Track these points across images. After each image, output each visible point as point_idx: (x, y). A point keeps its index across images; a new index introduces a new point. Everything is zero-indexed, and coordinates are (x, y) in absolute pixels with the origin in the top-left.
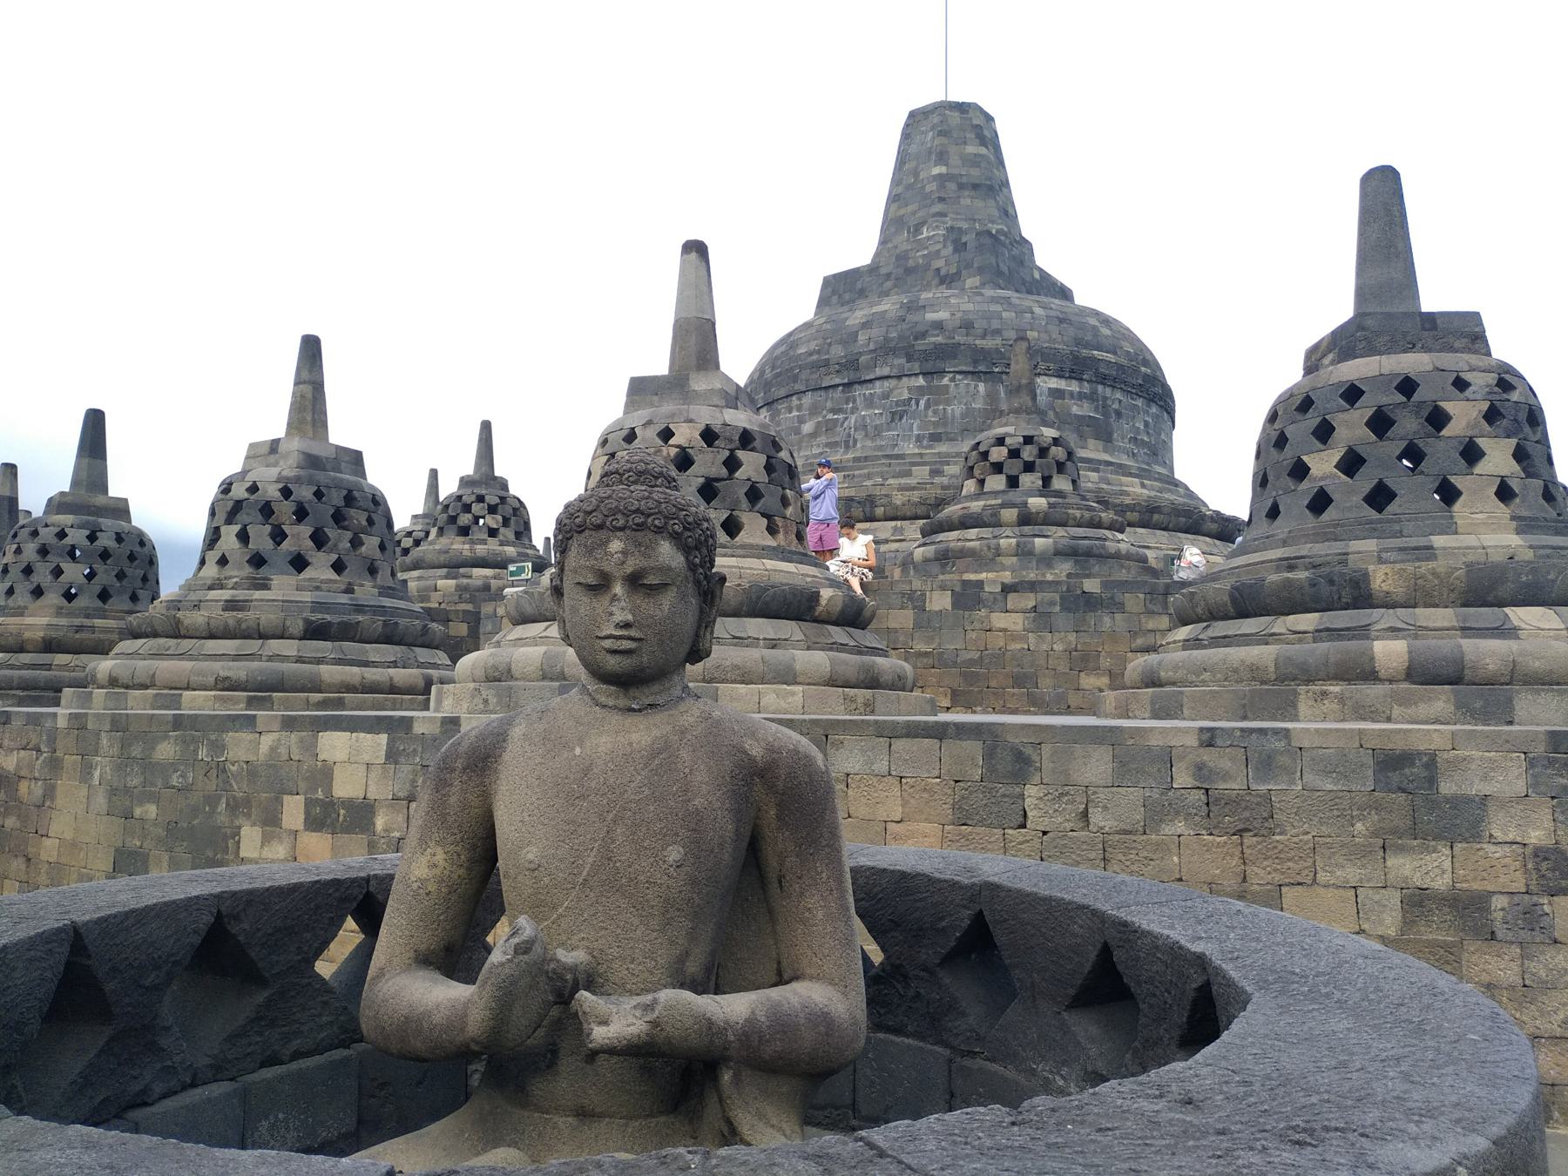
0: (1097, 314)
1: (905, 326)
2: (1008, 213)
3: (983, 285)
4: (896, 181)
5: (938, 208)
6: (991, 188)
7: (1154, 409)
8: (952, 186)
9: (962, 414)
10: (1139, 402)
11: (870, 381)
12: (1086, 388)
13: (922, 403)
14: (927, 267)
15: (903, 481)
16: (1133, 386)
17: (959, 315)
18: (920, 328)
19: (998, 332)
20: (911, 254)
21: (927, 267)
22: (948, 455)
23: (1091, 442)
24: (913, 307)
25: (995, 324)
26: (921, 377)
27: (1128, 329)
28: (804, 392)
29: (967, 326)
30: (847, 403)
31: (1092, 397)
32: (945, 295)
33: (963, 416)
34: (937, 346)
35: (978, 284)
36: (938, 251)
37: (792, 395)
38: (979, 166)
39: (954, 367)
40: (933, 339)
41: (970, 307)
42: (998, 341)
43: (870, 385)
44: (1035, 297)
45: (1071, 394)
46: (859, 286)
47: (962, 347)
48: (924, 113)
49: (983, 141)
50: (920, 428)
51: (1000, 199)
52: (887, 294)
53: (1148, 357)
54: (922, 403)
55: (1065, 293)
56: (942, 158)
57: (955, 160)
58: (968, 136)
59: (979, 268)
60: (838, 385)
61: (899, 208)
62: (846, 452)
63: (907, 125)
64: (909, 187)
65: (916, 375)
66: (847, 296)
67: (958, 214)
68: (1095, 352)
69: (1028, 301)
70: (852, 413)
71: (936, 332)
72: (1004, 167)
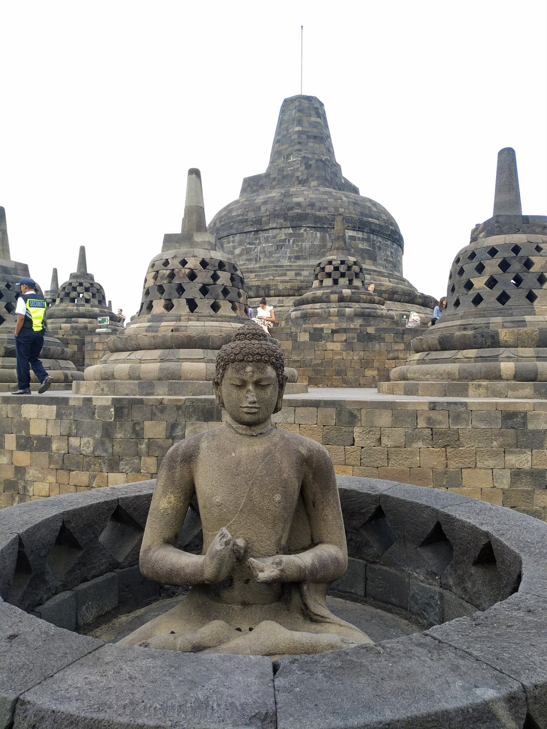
0: (370, 201)
2: (330, 151)
3: (319, 185)
4: (278, 133)
5: (297, 147)
6: (322, 138)
7: (395, 246)
8: (304, 137)
9: (309, 247)
10: (389, 243)
11: (267, 230)
13: (291, 241)
14: (292, 176)
15: (283, 278)
16: (386, 235)
17: (308, 200)
19: (326, 208)
20: (285, 169)
21: (292, 176)
22: (303, 266)
23: (367, 261)
24: (287, 195)
25: (325, 205)
26: (291, 228)
27: (384, 208)
28: (236, 234)
29: (312, 205)
30: (256, 240)
31: (368, 240)
32: (301, 190)
33: (310, 248)
34: (298, 214)
35: (317, 185)
36: (298, 168)
37: (230, 235)
39: (305, 224)
40: (296, 211)
41: (313, 196)
42: (326, 213)
43: (267, 232)
44: (343, 192)
45: (359, 238)
46: (260, 183)
50: (290, 253)
52: (273, 188)
53: (393, 222)
54: (291, 241)
55: (355, 190)
56: (300, 123)
57: (306, 124)
58: (312, 112)
59: (317, 177)
60: (251, 232)
61: (279, 146)
62: (256, 264)
63: (283, 106)
64: (284, 136)
65: (289, 227)
66: (255, 188)
69: (340, 194)
70: (259, 245)
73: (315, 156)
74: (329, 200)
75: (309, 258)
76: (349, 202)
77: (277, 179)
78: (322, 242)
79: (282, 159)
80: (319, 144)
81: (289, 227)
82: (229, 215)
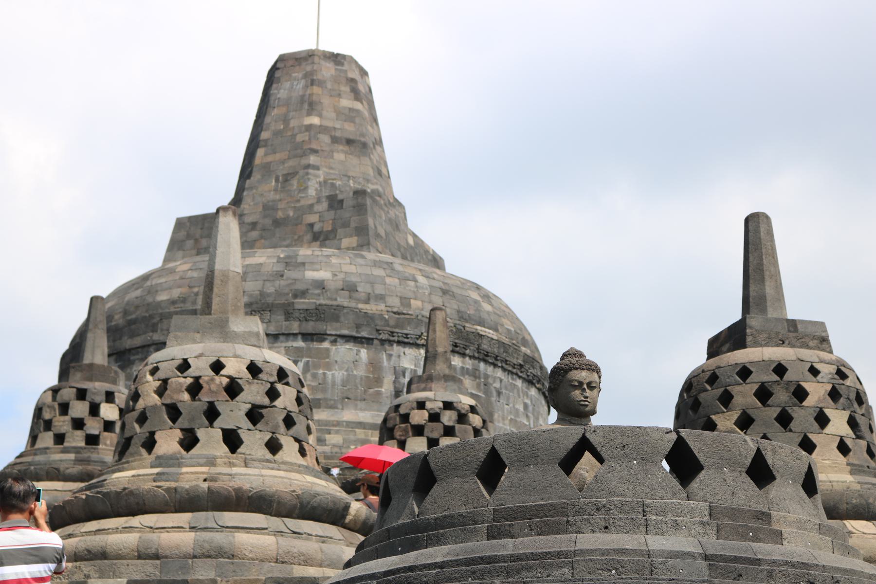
0: (478, 288)
1: (283, 283)
2: (381, 173)
6: (364, 145)
8: (325, 139)
9: (343, 381)
10: (519, 383)
12: (469, 363)
14: (298, 221)
16: (513, 367)
17: (341, 276)
18: (300, 286)
19: (381, 298)
20: (281, 205)
21: (298, 221)
24: (289, 263)
25: (379, 290)
27: (507, 307)
29: (350, 289)
31: (474, 374)
32: (325, 253)
35: (355, 245)
38: (354, 122)
39: (336, 329)
41: (352, 269)
42: (382, 307)
44: (415, 265)
47: (345, 311)
48: (297, 59)
49: (357, 95)
51: (375, 157)
53: (527, 337)
55: (436, 262)
57: (329, 113)
59: (357, 228)
65: (295, 335)
67: (331, 168)
68: (479, 328)
69: (410, 269)
71: (317, 291)
72: (377, 124)
73: (348, 181)
74: (388, 280)
75: (340, 406)
76: (431, 287)
77: (259, 226)
78: (373, 372)
79: (273, 183)
80: (359, 157)
81: (295, 335)
82: (150, 299)
